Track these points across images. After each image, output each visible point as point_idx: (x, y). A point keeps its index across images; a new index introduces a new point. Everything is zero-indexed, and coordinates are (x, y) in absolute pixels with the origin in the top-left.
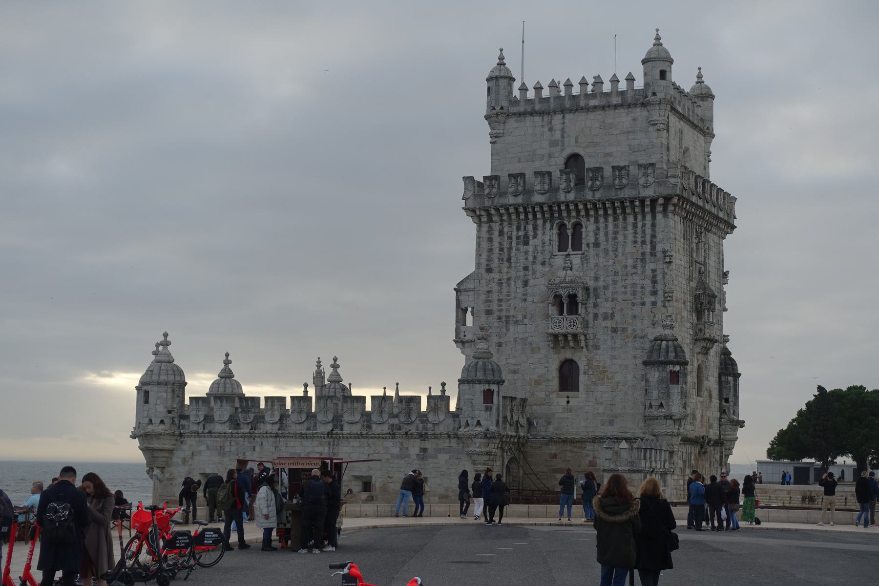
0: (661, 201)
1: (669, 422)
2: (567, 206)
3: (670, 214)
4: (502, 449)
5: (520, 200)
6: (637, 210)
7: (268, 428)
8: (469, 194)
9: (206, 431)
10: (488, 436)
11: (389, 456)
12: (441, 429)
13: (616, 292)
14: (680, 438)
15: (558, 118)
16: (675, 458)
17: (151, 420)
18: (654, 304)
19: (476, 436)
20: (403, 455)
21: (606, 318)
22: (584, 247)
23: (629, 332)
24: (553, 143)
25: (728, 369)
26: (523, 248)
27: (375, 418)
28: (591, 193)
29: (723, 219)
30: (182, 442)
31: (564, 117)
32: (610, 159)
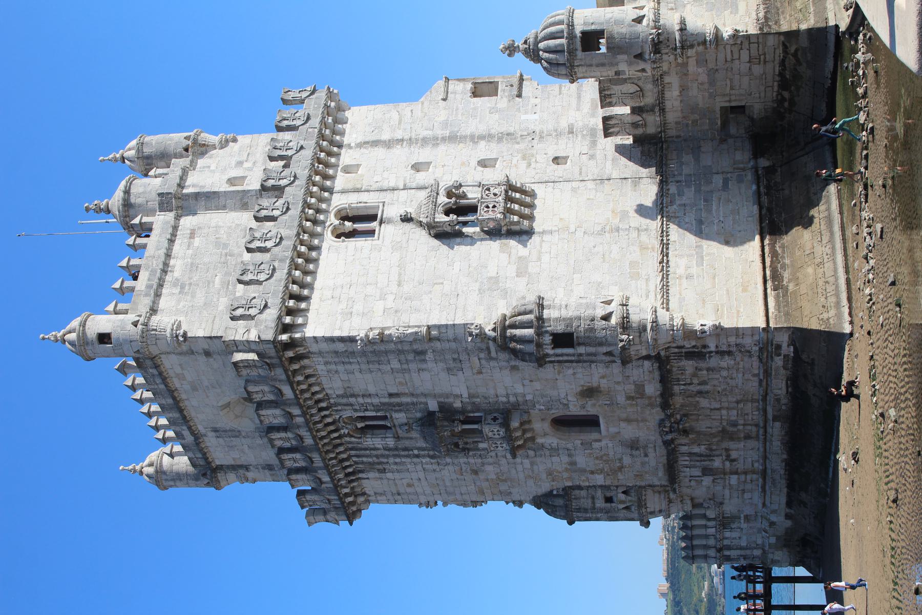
16: (700, 493)
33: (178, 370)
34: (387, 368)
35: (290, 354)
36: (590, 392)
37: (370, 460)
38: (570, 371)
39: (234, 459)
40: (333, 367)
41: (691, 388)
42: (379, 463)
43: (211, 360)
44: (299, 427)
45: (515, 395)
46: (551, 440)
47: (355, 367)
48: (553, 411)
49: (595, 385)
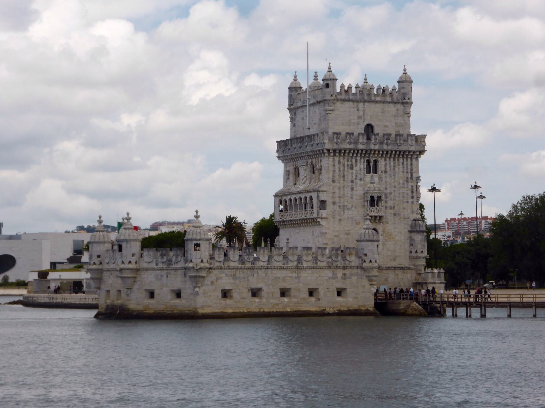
5: (352, 146)
7: (261, 264)
9: (226, 266)
11: (327, 278)
12: (353, 264)
15: (361, 105)
18: (412, 202)
19: (375, 268)
20: (334, 277)
21: (391, 208)
22: (379, 173)
23: (402, 216)
24: (359, 117)
26: (350, 171)
28: (386, 146)
30: (210, 272)
32: (387, 129)
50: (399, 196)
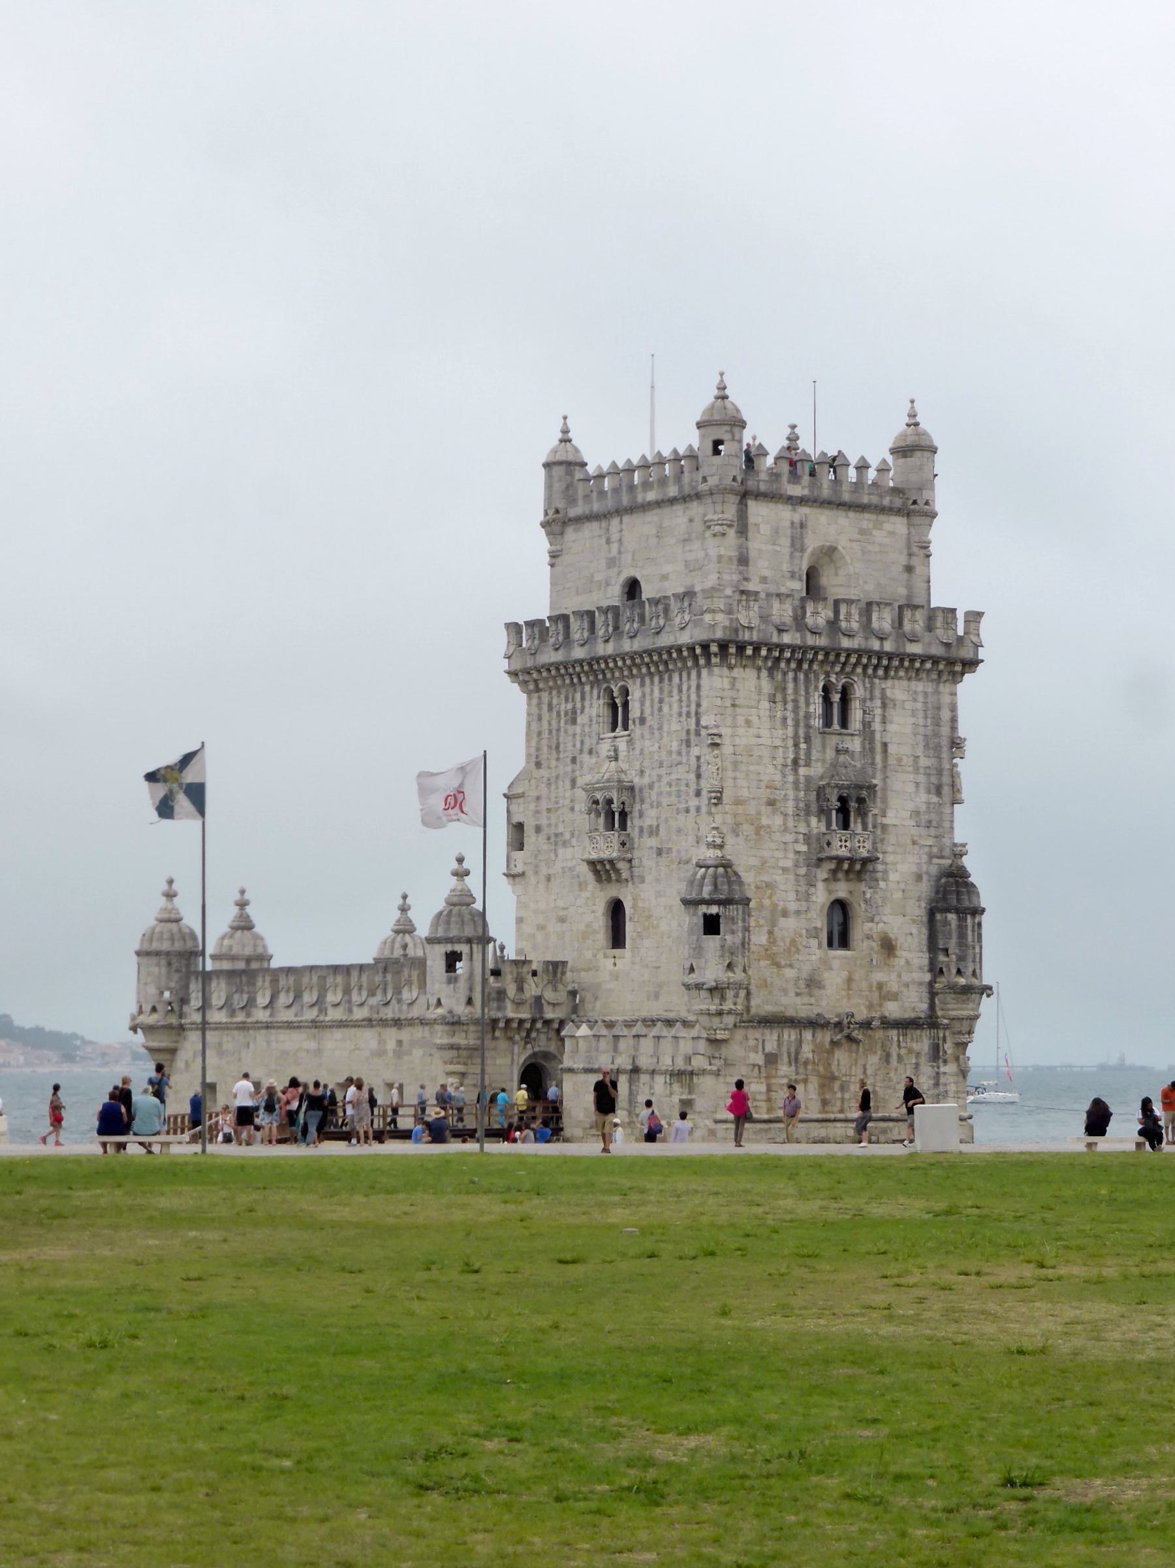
0: (698, 651)
1: (704, 994)
2: (607, 663)
3: (715, 669)
4: (511, 1039)
6: (679, 665)
7: (261, 1015)
8: (512, 648)
10: (454, 1023)
12: (415, 1012)
13: (661, 793)
14: (730, 1020)
15: (615, 522)
17: (141, 1007)
18: (698, 809)
23: (674, 854)
24: (612, 562)
25: (952, 899)
26: (570, 728)
27: (355, 997)
29: (920, 656)
31: (621, 522)
33: (888, 527)
34: (920, 752)
35: (958, 668)
36: (888, 947)
37: (790, 691)
38: (914, 931)
39: (757, 525)
40: (921, 699)
41: (895, 1045)
42: (785, 703)
43: (901, 569)
44: (867, 639)
45: (885, 872)
46: (821, 897)
47: (921, 721)
48: (863, 906)
49: (898, 953)
50: (669, 794)
